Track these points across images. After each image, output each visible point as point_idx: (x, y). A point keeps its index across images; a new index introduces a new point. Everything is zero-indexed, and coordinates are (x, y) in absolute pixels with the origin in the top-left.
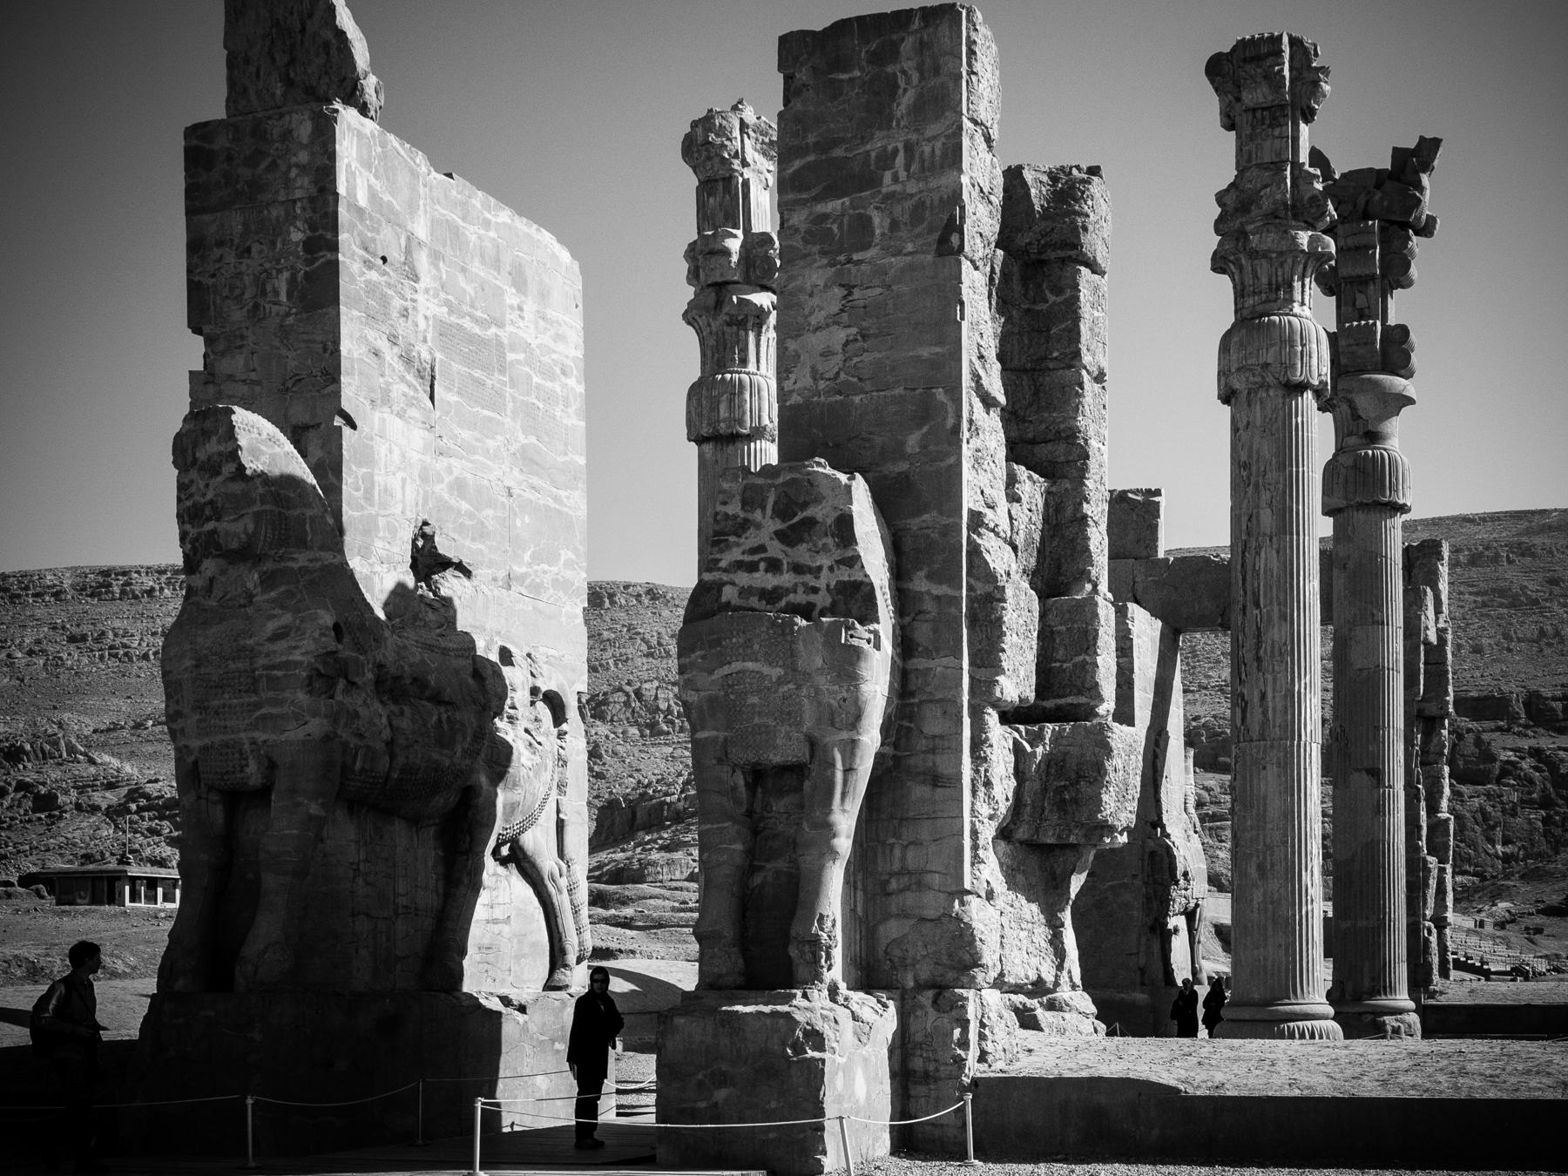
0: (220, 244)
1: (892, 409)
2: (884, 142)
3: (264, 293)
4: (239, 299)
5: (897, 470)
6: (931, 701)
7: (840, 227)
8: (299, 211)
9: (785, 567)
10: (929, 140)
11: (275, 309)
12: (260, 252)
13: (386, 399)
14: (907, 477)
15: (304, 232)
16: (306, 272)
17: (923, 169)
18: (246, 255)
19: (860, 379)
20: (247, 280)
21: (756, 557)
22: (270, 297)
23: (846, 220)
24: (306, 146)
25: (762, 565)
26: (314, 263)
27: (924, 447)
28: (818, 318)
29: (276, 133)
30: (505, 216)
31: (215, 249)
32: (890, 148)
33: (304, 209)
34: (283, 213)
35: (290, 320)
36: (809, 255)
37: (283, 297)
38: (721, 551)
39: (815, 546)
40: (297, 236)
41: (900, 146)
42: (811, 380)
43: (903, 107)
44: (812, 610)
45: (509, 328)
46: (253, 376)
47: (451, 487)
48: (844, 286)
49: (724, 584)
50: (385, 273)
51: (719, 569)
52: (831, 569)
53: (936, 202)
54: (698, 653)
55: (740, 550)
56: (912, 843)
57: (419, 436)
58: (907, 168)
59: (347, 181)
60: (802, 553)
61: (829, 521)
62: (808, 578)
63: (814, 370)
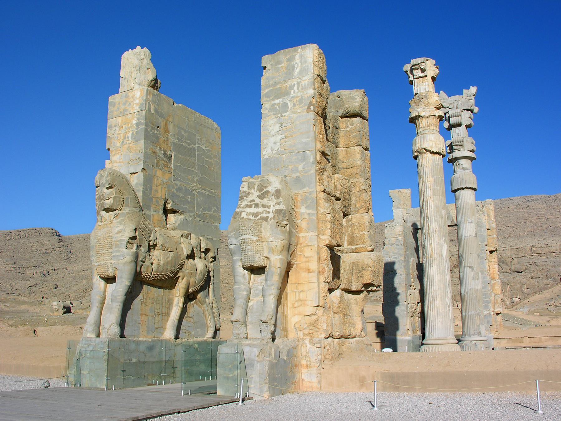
0: (116, 126)
1: (294, 158)
2: (291, 82)
3: (125, 138)
5: (296, 175)
6: (307, 246)
8: (135, 116)
9: (260, 206)
10: (304, 81)
11: (128, 142)
12: (125, 127)
13: (157, 165)
14: (299, 178)
17: (302, 89)
19: (285, 150)
20: (121, 135)
21: (252, 203)
22: (127, 139)
23: (280, 104)
24: (138, 98)
25: (253, 206)
27: (304, 168)
30: (197, 114)
32: (293, 84)
33: (137, 115)
35: (131, 145)
36: (270, 115)
37: (130, 139)
38: (242, 202)
39: (269, 199)
40: (134, 122)
41: (296, 83)
42: (271, 151)
43: (296, 73)
44: (268, 219)
45: (197, 145)
46: (121, 160)
47: (177, 190)
49: (242, 212)
50: (158, 131)
52: (274, 206)
53: (306, 98)
55: (247, 201)
56: (302, 291)
57: (167, 176)
58: (298, 89)
59: (148, 106)
60: (265, 201)
61: (273, 191)
62: (267, 209)
63: (272, 148)
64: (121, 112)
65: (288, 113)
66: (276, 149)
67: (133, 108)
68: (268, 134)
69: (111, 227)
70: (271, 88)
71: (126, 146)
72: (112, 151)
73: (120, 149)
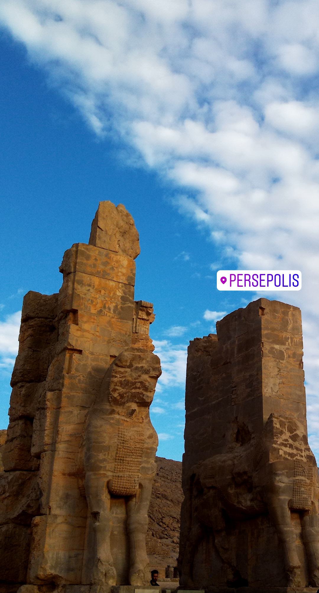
0: (89, 285)
3: (105, 307)
4: (95, 305)
7: (277, 352)
11: (108, 314)
12: (105, 294)
15: (121, 293)
16: (121, 306)
18: (99, 293)
19: (283, 395)
20: (99, 301)
26: (125, 305)
28: (272, 374)
29: (115, 259)
31: (87, 286)
33: (122, 286)
34: (114, 285)
37: (112, 311)
38: (278, 439)
40: (119, 293)
46: (98, 334)
48: (278, 368)
51: (278, 444)
54: (285, 471)
63: (271, 388)
64: (98, 272)
65: (285, 361)
66: (276, 391)
67: (117, 275)
68: (268, 374)
69: (142, 428)
70: (269, 331)
71: (108, 319)
72: (83, 316)
73: (96, 318)
